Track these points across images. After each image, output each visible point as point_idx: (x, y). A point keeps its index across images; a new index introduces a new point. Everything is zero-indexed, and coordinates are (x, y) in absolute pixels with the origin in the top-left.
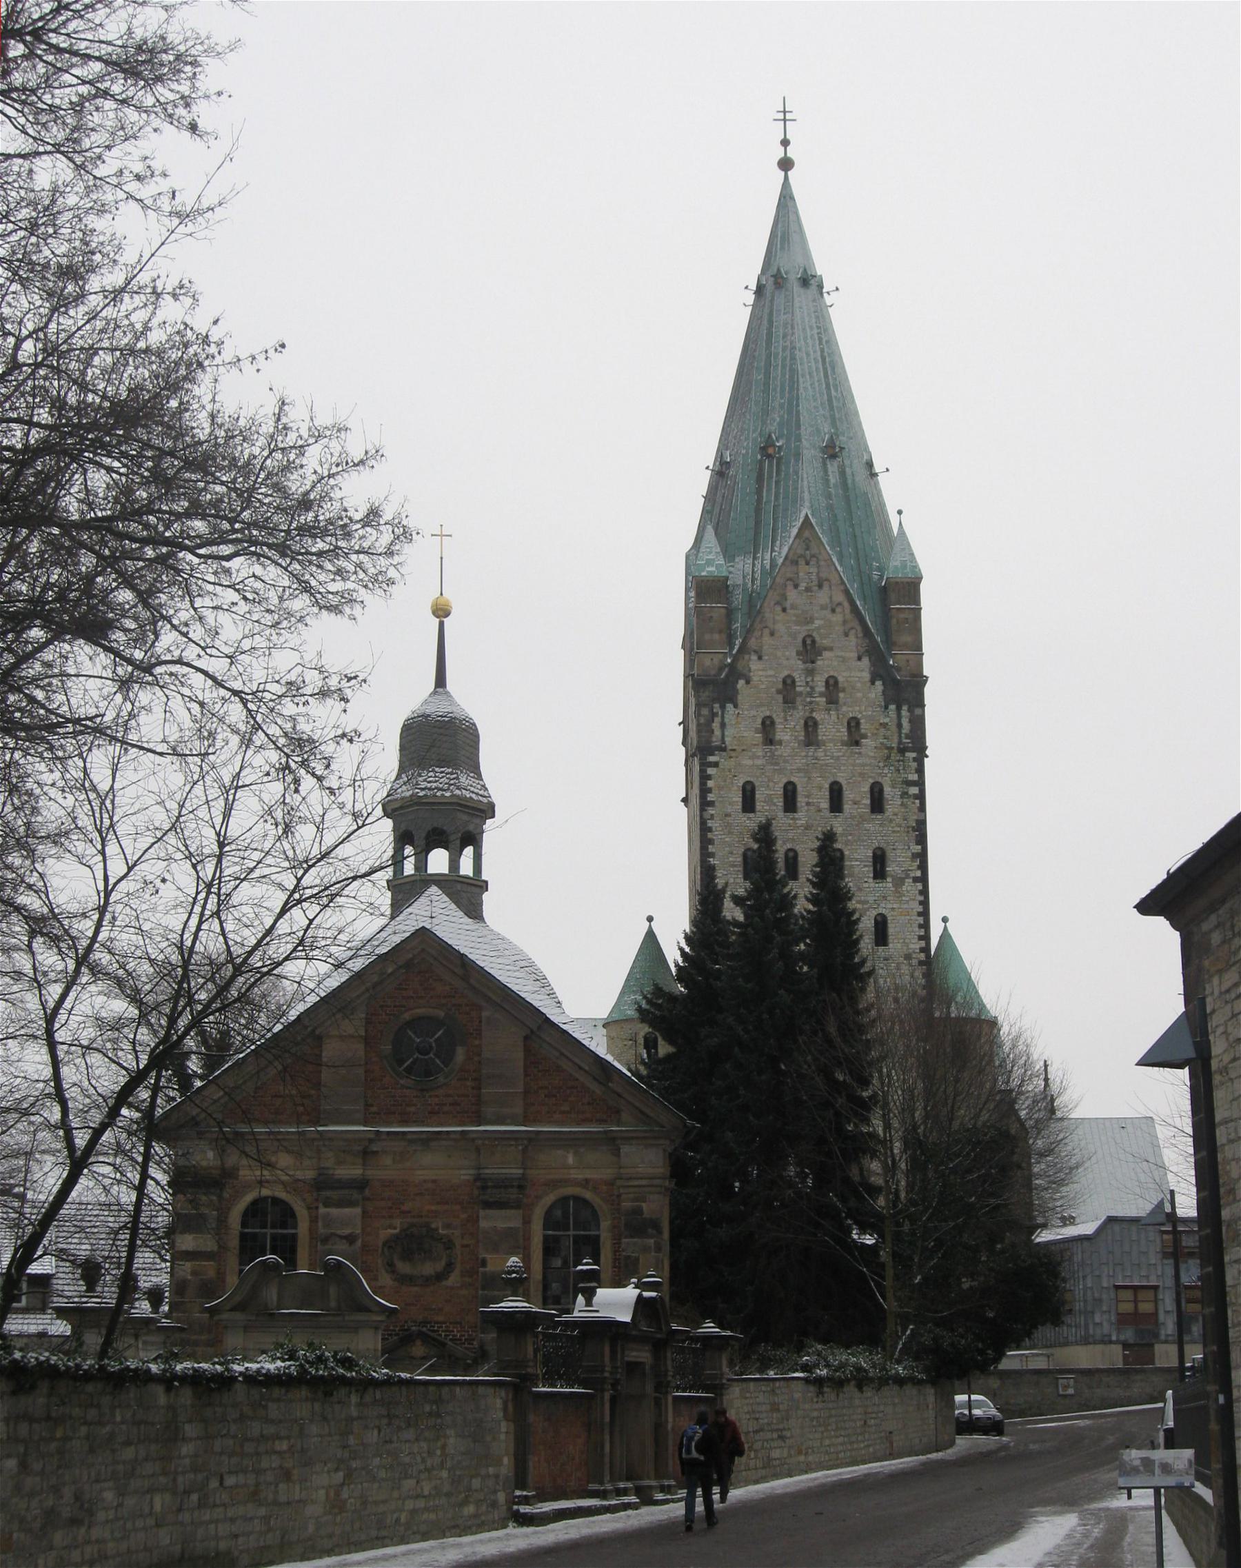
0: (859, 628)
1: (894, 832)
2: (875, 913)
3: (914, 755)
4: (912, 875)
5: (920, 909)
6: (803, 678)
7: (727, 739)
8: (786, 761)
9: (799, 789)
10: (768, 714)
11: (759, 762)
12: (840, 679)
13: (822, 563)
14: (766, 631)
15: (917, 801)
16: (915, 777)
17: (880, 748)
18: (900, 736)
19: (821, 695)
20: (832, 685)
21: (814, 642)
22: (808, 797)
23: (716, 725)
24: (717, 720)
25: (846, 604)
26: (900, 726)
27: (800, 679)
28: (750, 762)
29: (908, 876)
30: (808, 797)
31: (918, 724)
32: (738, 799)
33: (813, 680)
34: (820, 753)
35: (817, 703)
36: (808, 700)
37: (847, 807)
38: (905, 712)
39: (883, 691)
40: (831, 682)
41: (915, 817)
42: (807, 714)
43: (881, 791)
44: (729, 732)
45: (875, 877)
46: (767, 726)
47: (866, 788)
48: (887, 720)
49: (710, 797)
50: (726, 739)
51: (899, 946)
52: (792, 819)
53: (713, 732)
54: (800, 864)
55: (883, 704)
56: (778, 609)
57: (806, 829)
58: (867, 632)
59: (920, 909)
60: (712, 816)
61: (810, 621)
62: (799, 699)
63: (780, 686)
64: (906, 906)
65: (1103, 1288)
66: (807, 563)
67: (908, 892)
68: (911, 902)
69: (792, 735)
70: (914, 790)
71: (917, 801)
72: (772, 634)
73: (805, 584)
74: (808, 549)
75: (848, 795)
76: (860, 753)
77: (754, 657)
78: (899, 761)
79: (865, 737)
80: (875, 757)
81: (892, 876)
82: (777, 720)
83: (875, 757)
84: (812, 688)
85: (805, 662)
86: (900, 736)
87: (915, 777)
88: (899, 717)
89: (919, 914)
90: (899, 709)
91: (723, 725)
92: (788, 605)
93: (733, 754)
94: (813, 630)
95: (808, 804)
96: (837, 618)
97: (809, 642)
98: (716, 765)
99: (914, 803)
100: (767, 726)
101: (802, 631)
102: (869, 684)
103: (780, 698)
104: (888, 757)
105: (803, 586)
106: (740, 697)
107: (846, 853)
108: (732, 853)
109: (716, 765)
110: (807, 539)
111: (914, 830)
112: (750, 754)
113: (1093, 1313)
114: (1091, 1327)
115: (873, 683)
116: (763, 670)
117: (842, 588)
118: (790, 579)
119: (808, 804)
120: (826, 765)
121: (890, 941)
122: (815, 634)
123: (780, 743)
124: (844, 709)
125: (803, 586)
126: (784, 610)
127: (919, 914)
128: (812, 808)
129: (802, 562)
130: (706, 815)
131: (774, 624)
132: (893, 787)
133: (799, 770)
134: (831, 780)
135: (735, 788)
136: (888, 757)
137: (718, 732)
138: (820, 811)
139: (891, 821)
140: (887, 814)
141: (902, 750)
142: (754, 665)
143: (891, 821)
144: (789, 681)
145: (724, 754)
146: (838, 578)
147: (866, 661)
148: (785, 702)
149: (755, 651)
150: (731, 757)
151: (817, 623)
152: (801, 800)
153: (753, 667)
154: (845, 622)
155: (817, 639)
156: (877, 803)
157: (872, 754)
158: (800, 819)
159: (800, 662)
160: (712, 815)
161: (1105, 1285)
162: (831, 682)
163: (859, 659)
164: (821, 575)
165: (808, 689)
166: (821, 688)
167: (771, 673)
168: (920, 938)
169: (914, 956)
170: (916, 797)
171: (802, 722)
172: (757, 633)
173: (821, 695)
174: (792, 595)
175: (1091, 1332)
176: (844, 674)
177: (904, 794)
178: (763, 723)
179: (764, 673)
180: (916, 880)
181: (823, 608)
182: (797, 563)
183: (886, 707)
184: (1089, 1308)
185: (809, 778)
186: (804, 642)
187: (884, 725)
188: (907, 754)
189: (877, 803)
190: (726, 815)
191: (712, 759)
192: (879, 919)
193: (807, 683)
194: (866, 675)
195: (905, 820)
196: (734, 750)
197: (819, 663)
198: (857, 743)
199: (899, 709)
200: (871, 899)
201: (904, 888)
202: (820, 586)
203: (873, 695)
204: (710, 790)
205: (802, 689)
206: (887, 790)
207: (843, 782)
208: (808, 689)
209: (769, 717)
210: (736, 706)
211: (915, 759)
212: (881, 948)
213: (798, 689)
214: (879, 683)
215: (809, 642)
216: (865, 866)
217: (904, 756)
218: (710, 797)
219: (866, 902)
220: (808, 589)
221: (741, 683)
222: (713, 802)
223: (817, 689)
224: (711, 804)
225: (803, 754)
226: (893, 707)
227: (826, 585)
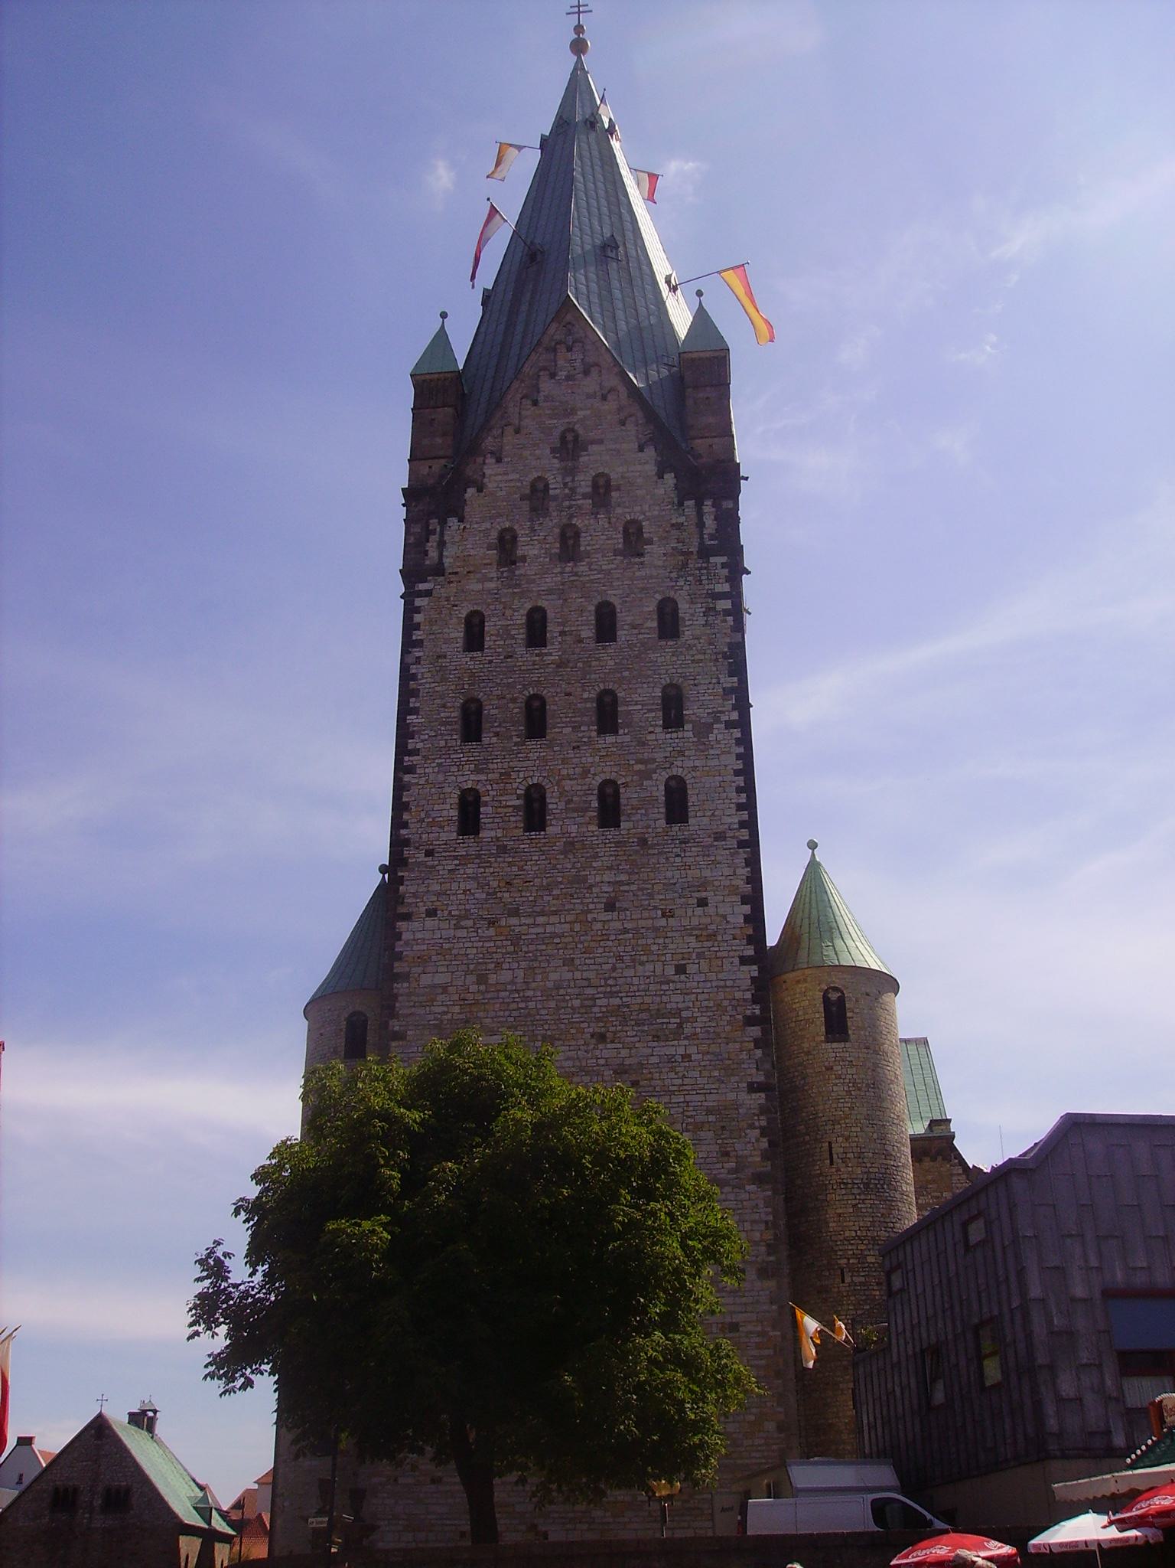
0: (640, 414)
1: (693, 661)
2: (665, 775)
3: (724, 559)
4: (724, 718)
5: (739, 765)
6: (559, 479)
7: (447, 561)
8: (533, 581)
9: (550, 615)
10: (507, 525)
11: (492, 585)
12: (613, 476)
13: (588, 347)
14: (509, 430)
15: (730, 619)
16: (726, 588)
17: (672, 555)
18: (701, 538)
19: (585, 496)
20: (602, 491)
21: (576, 438)
22: (563, 624)
23: (432, 546)
24: (434, 539)
25: (623, 391)
26: (701, 525)
27: (555, 481)
28: (479, 587)
29: (717, 720)
30: (563, 624)
31: (729, 522)
32: (457, 633)
33: (573, 480)
34: (582, 567)
35: (580, 507)
36: (567, 503)
37: (622, 634)
38: (708, 507)
39: (676, 486)
40: (602, 481)
41: (728, 640)
42: (565, 521)
43: (675, 610)
44: (450, 552)
45: (666, 726)
46: (506, 546)
47: (652, 606)
48: (682, 519)
49: (417, 635)
50: (445, 560)
51: (706, 820)
52: (537, 655)
53: (426, 553)
54: (549, 714)
55: (676, 500)
56: (527, 402)
57: (558, 666)
58: (651, 416)
59: (739, 765)
60: (418, 660)
61: (573, 411)
62: (553, 504)
63: (528, 491)
64: (716, 762)
65: (1073, 1300)
66: (569, 349)
67: (718, 742)
68: (723, 757)
69: (541, 548)
70: (726, 604)
71: (730, 619)
72: (517, 431)
73: (565, 373)
74: (570, 333)
75: (624, 618)
76: (642, 563)
77: (490, 460)
78: (700, 569)
79: (650, 542)
80: (665, 567)
81: (691, 722)
82: (520, 532)
83: (665, 567)
84: (573, 490)
85: (561, 460)
86: (701, 538)
87: (726, 588)
88: (700, 514)
89: (737, 773)
90: (699, 506)
91: (442, 544)
92: (541, 398)
93: (453, 578)
94: (575, 423)
95: (562, 633)
96: (610, 406)
97: (570, 437)
98: (428, 593)
99: (726, 621)
100: (506, 546)
101: (559, 425)
102: (656, 478)
103: (526, 506)
104: (685, 565)
105: (562, 375)
106: (467, 509)
107: (621, 694)
108: (444, 706)
109: (428, 593)
110: (569, 323)
111: (725, 657)
112: (478, 576)
113: (1052, 1368)
114: (1050, 1409)
115: (660, 476)
116: (505, 474)
117: (616, 370)
118: (544, 369)
119: (562, 633)
120: (592, 581)
121: (690, 814)
122: (577, 427)
123: (524, 559)
124: (619, 510)
125: (562, 375)
126: (535, 403)
127: (737, 773)
128: (568, 638)
129: (562, 349)
130: (410, 659)
131: (520, 420)
132: (692, 603)
133: (550, 592)
134: (599, 599)
135: (455, 620)
136: (685, 565)
137: (433, 554)
138: (581, 641)
139: (690, 647)
140: (683, 640)
141: (705, 553)
142: (491, 469)
143: (690, 647)
144: (541, 486)
145: (441, 579)
146: (610, 360)
147: (650, 452)
148: (533, 509)
149: (492, 453)
150: (449, 583)
151: (581, 414)
152: (553, 629)
153: (488, 472)
154: (620, 409)
155: (581, 432)
156: (669, 623)
157: (660, 563)
158: (551, 654)
159: (556, 461)
160: (419, 658)
161: (1079, 1291)
162: (602, 481)
163: (641, 449)
164: (587, 359)
165: (567, 491)
166: (584, 483)
167: (516, 476)
168: (740, 807)
169: (730, 834)
170: (727, 613)
171: (557, 531)
172: (496, 432)
173: (585, 496)
174: (546, 386)
175: (1052, 1423)
176: (620, 469)
177: (709, 611)
178: (501, 538)
179: (505, 477)
180: (729, 725)
181: (589, 396)
182: (555, 350)
183: (681, 504)
184: (1041, 1359)
185: (566, 600)
186: (563, 438)
187: (678, 526)
188: (712, 559)
189: (669, 623)
190: (439, 657)
191: (422, 587)
192: (673, 783)
193: (565, 484)
194: (651, 469)
195: (710, 644)
196: (456, 573)
197: (581, 459)
198: (641, 555)
199: (699, 506)
200: (659, 756)
201: (712, 737)
202: (586, 372)
203: (662, 491)
204: (417, 627)
205: (558, 491)
206: (683, 606)
207: (616, 601)
208: (567, 491)
209: (510, 530)
210: (461, 520)
211: (724, 565)
212: (676, 827)
213: (551, 492)
214: (670, 478)
215: (570, 437)
216: (650, 711)
217: (708, 562)
218: (417, 635)
219: (654, 760)
220: (569, 378)
221: (471, 492)
222: (421, 640)
223: (580, 490)
224: (419, 643)
225: (559, 570)
226: (691, 503)
227: (594, 371)
